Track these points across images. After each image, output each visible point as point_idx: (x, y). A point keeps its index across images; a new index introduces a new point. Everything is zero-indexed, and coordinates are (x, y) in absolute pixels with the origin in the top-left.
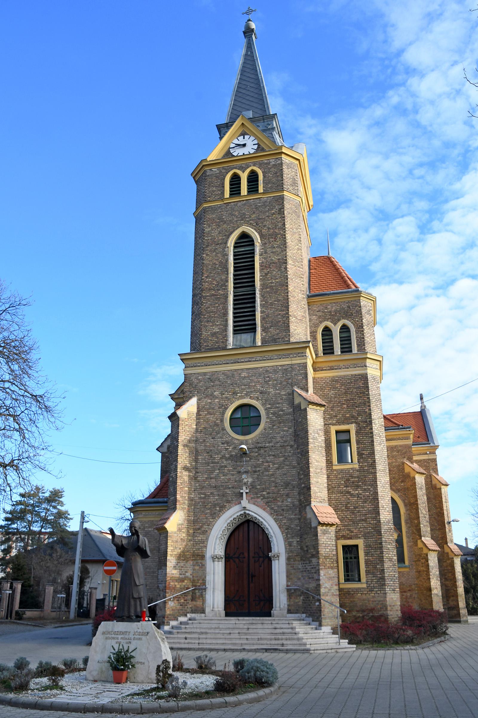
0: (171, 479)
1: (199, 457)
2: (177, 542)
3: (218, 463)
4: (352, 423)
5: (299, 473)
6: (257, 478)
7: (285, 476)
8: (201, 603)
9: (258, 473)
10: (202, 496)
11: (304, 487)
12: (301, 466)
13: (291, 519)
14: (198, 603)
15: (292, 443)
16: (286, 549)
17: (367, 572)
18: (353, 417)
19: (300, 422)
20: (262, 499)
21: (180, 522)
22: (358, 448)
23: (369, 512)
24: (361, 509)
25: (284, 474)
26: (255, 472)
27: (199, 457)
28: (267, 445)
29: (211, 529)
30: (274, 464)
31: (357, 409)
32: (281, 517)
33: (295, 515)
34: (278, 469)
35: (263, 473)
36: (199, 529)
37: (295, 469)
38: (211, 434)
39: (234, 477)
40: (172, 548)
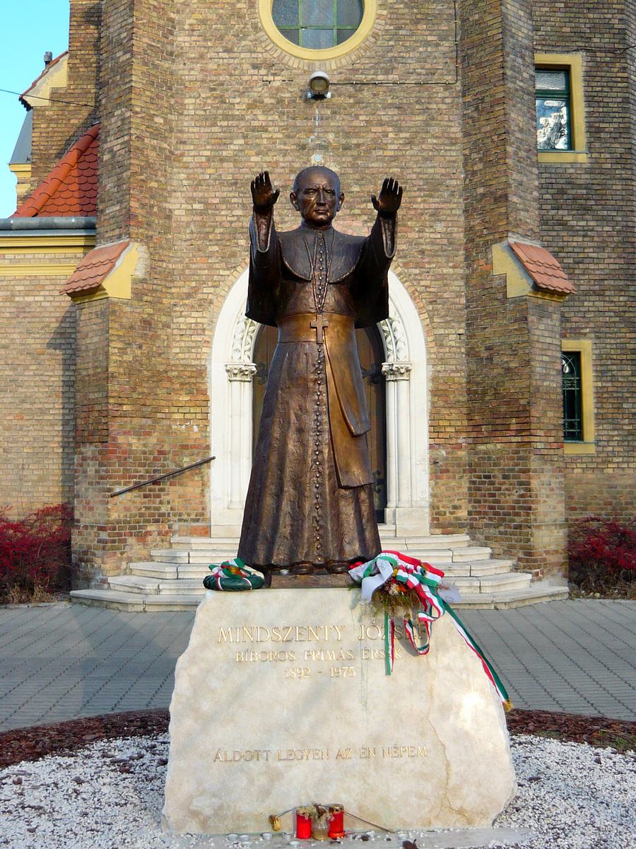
0: (106, 157)
1: (186, 101)
2: (132, 327)
3: (242, 118)
4: (577, 50)
5: (467, 158)
6: (353, 166)
7: (429, 164)
8: (198, 491)
9: (355, 153)
10: (196, 206)
11: (484, 195)
12: (474, 138)
13: (442, 277)
14: (189, 489)
15: (449, 78)
16: (429, 352)
17: (600, 418)
18: (580, 34)
19: (477, 23)
20: (366, 222)
21: (140, 274)
22: (589, 114)
23: (612, 275)
24: (592, 266)
25: (426, 159)
26: (347, 148)
27: (186, 101)
28: (381, 77)
29: (224, 297)
30: (399, 129)
31: (591, 16)
32: (417, 271)
33: (454, 267)
34: (410, 142)
35: (368, 151)
36: (189, 296)
37: (457, 147)
38: (221, 38)
39: (289, 158)
40: (120, 345)
